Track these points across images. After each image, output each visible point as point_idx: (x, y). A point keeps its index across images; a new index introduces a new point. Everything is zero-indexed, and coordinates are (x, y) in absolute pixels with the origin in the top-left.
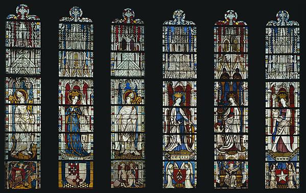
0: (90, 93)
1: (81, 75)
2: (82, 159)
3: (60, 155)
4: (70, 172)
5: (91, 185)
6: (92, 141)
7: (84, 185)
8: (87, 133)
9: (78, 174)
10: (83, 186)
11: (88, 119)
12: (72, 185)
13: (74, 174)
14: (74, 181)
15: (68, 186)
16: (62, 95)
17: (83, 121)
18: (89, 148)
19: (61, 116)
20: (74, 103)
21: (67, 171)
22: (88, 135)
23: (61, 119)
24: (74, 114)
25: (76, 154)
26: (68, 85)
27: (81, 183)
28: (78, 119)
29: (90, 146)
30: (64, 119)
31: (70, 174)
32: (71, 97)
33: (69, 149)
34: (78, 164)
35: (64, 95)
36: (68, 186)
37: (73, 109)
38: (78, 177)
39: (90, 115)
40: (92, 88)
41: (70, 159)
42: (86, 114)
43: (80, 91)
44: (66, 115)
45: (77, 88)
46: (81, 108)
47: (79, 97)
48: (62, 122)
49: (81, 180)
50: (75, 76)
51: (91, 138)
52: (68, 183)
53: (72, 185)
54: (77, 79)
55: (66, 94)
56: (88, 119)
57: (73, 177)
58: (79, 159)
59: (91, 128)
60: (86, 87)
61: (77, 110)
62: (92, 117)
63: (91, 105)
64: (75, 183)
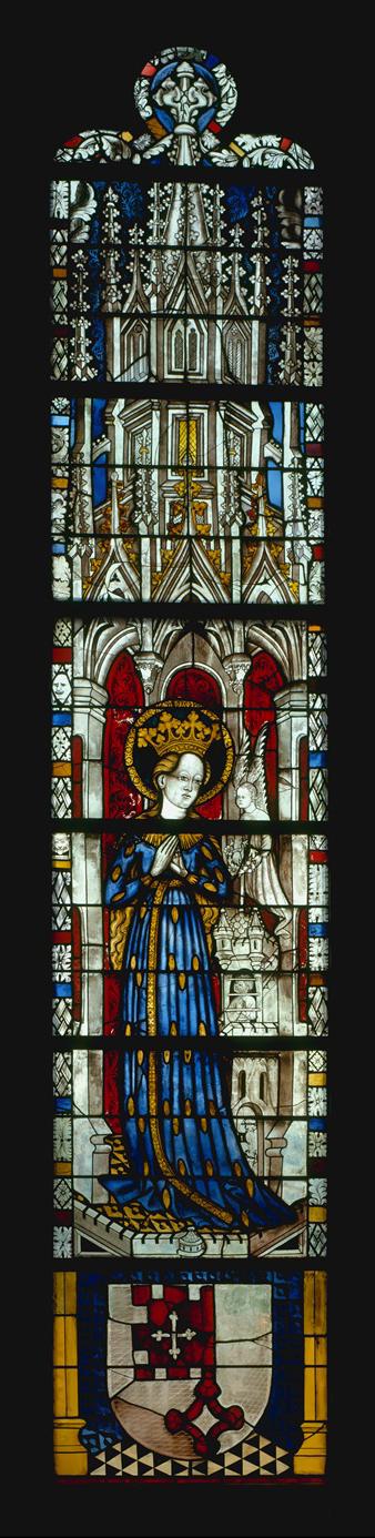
0: (299, 725)
1: (228, 587)
2: (237, 1249)
3: (67, 1218)
4: (142, 1357)
5: (310, 1459)
6: (318, 1108)
7: (254, 1459)
8: (277, 1047)
9: (210, 1369)
10: (248, 1468)
11: (287, 932)
12: (159, 1459)
13: (177, 1372)
14: (177, 1422)
15: (127, 1461)
16: (77, 743)
17: (243, 949)
18: (294, 1163)
19: (74, 912)
20: (172, 811)
21: (119, 1348)
22: (285, 1065)
23: (74, 938)
24: (178, 898)
25: (188, 1214)
26: (125, 664)
27: (231, 1438)
28: (206, 932)
29: (297, 1147)
30: (92, 932)
31: (144, 1373)
32: (148, 761)
33: (133, 1173)
34: (208, 1294)
35: (93, 746)
36: (127, 1461)
37: (162, 856)
38: (207, 1393)
39: (299, 900)
40: (314, 685)
41: (145, 1248)
42: (270, 896)
43: (219, 709)
44: (108, 907)
45: (195, 690)
46: (232, 849)
47: (215, 758)
48: (77, 957)
49: (232, 1418)
50: (178, 594)
51: (307, 1088)
52: (128, 1441)
53: (159, 1459)
54: (193, 616)
55: (113, 737)
56: (287, 932)
57: (168, 1394)
58: (214, 1249)
59: (304, 1003)
60: (268, 679)
61: (200, 859)
62: (317, 915)
63: (304, 826)
64: (184, 1442)
